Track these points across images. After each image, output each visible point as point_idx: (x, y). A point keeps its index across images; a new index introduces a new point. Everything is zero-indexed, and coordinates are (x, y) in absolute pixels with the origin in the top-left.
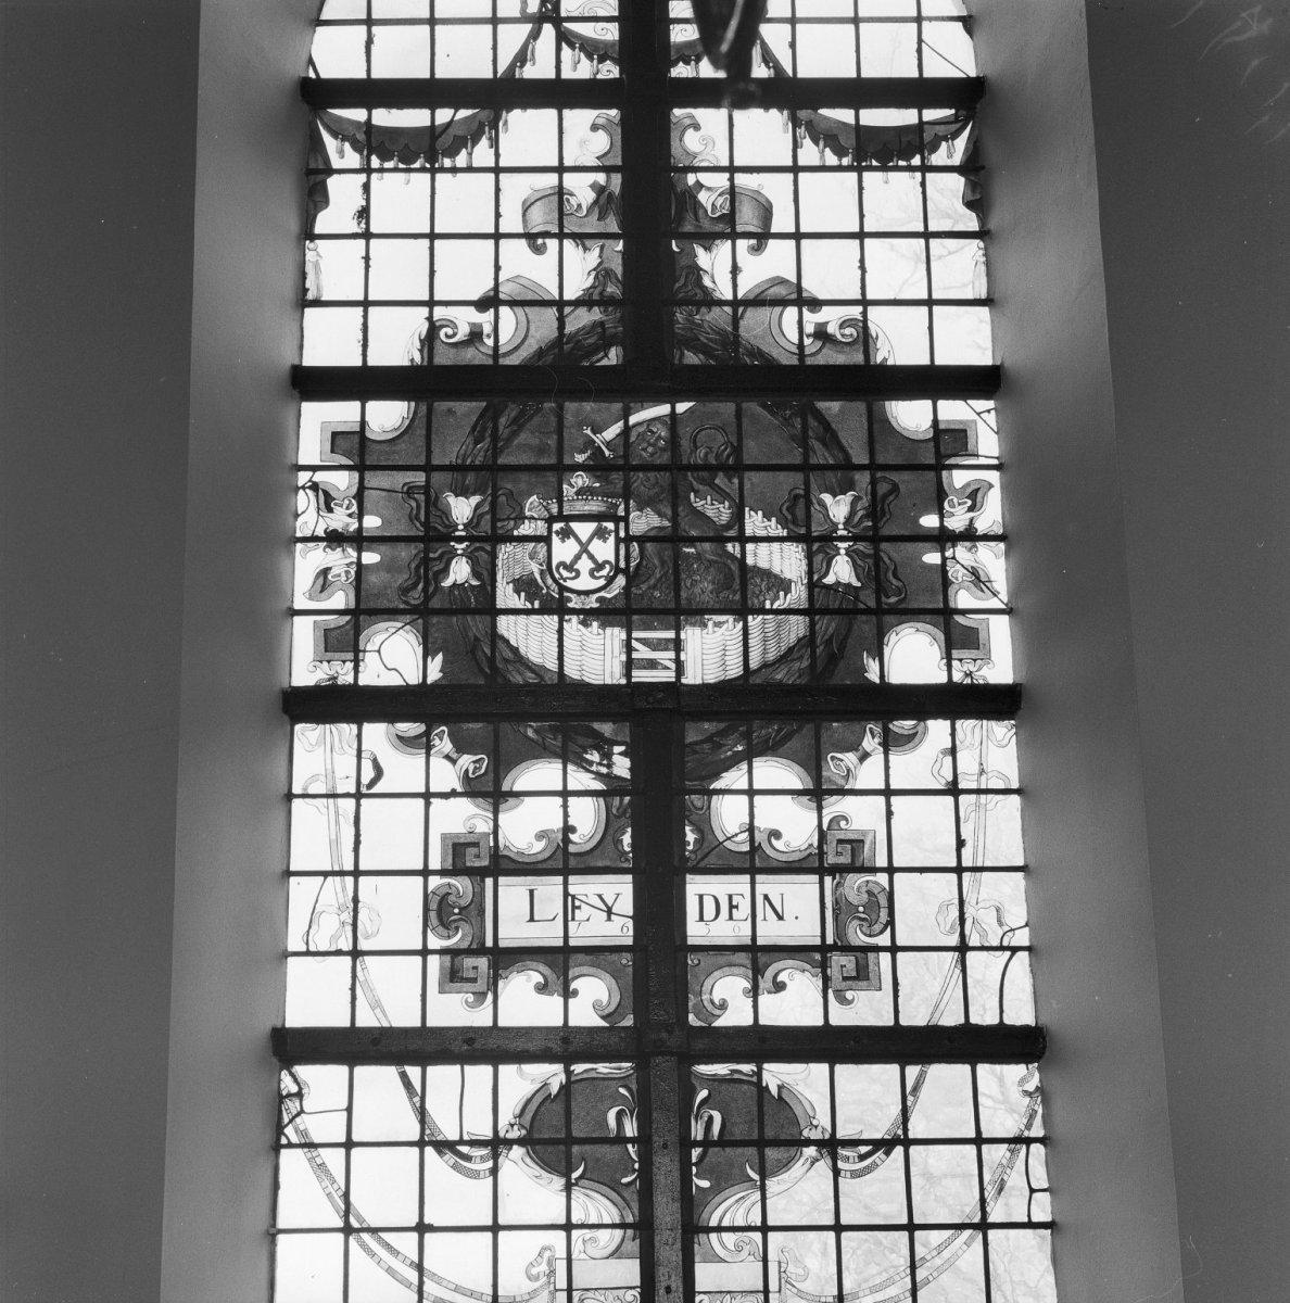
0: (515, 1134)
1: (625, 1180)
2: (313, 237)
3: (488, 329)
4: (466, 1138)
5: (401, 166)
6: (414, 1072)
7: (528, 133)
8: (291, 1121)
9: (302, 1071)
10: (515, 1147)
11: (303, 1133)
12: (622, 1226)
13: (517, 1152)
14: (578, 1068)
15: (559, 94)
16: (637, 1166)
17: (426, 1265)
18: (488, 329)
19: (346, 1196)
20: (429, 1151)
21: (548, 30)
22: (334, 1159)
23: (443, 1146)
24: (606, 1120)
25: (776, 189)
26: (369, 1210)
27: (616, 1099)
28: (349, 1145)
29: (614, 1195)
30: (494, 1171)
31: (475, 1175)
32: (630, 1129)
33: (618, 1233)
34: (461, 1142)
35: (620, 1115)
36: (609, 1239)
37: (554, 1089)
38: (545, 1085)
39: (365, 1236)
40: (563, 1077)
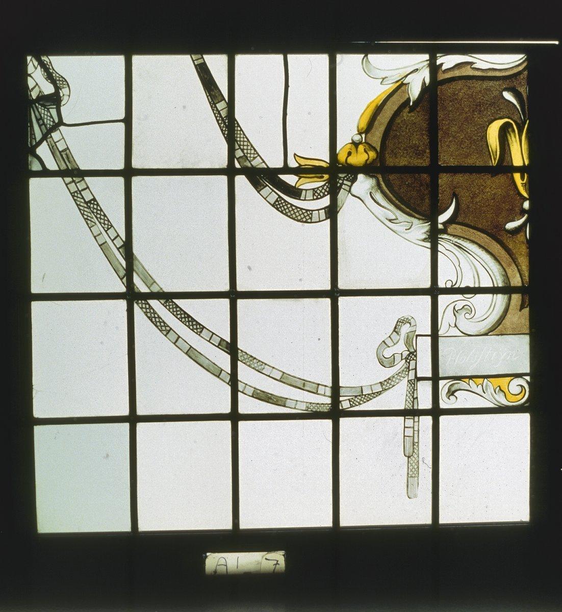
0: (360, 158)
1: (510, 226)
4: (293, 164)
6: (217, 63)
8: (45, 137)
9: (61, 63)
10: (361, 177)
11: (64, 155)
12: (507, 290)
13: (363, 184)
14: (448, 61)
16: (526, 205)
17: (240, 345)
19: (127, 248)
20: (241, 181)
22: (108, 194)
23: (262, 177)
24: (484, 138)
26: (161, 268)
27: (498, 108)
28: (128, 173)
29: (496, 248)
30: (332, 212)
31: (305, 217)
32: (519, 155)
33: (500, 300)
34: (286, 170)
35: (504, 132)
36: (488, 307)
37: (415, 92)
38: (401, 86)
39: (155, 304)
40: (425, 75)
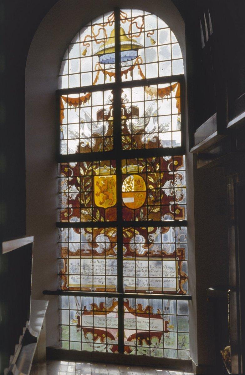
2: (62, 125)
3: (90, 143)
5: (74, 107)
7: (97, 96)
15: (103, 88)
18: (90, 143)
21: (101, 72)
25: (140, 106)
